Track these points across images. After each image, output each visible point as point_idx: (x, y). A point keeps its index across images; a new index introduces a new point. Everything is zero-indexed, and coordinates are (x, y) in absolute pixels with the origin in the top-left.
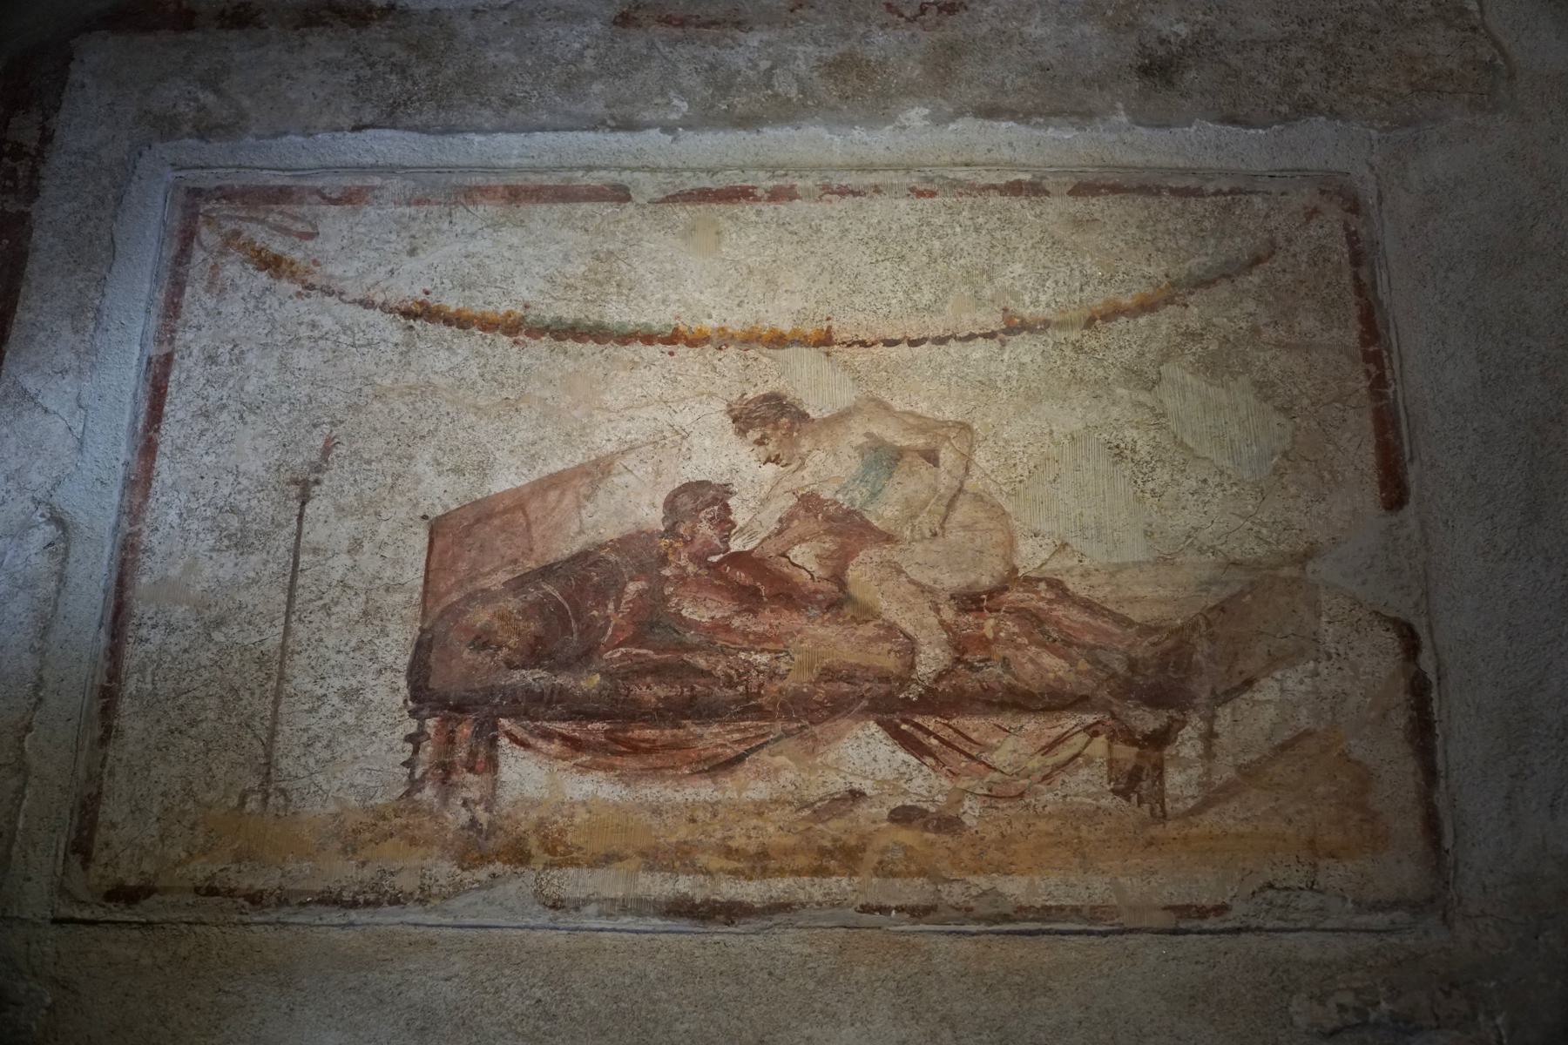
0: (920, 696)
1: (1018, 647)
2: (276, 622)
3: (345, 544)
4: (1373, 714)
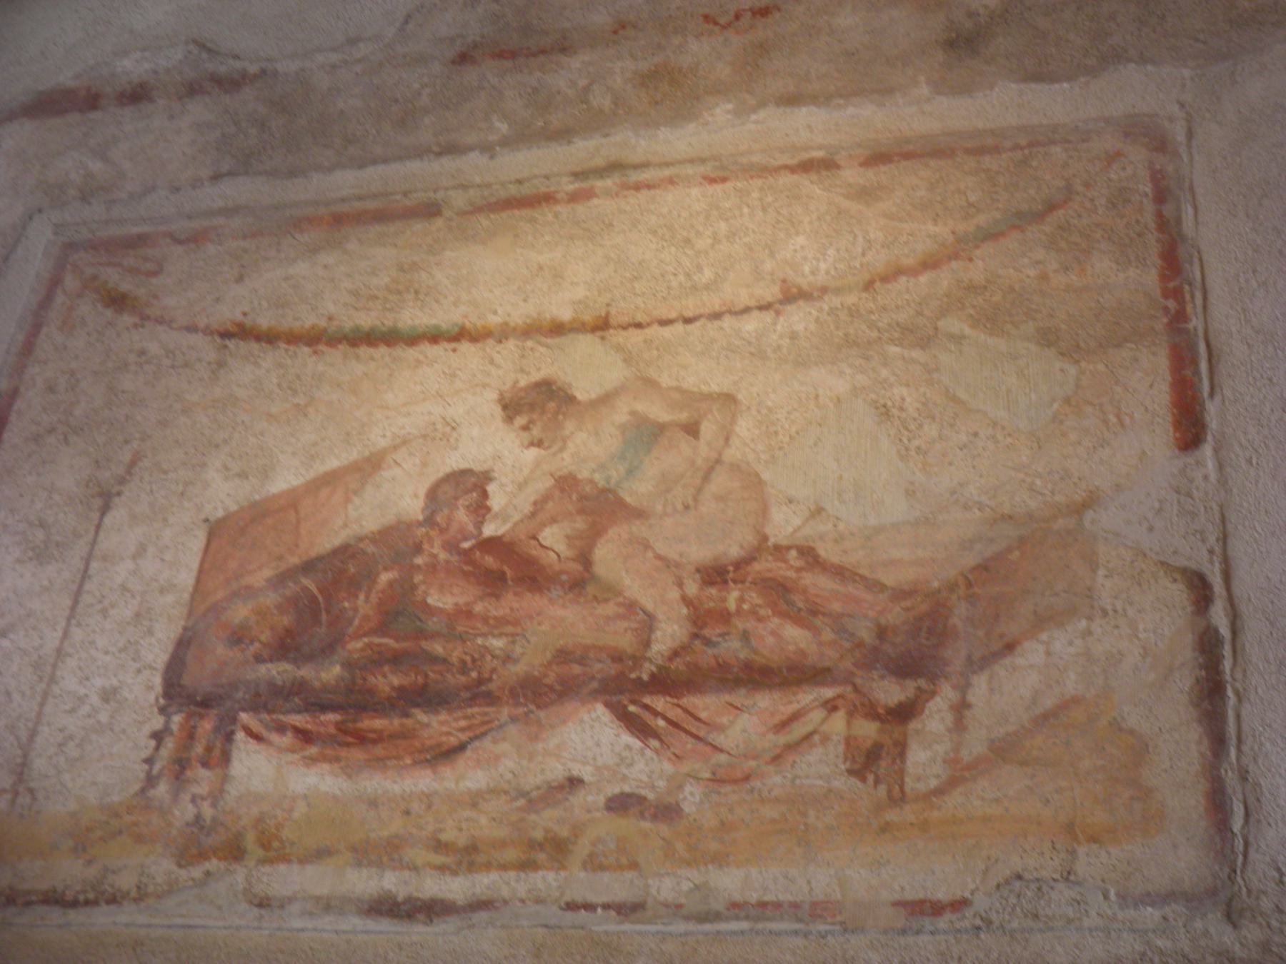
0: (653, 676)
1: (760, 620)
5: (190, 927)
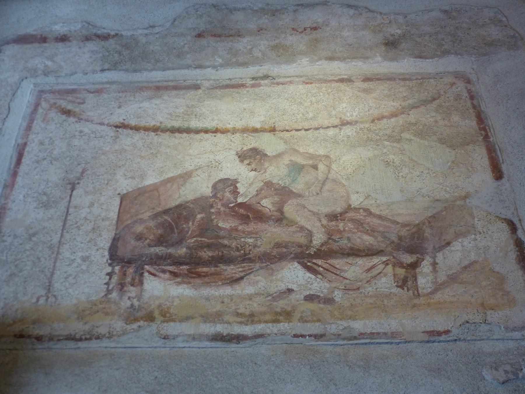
0: (315, 252)
1: (354, 233)
2: (58, 233)
3: (88, 204)
4: (501, 254)
5: (133, 347)
